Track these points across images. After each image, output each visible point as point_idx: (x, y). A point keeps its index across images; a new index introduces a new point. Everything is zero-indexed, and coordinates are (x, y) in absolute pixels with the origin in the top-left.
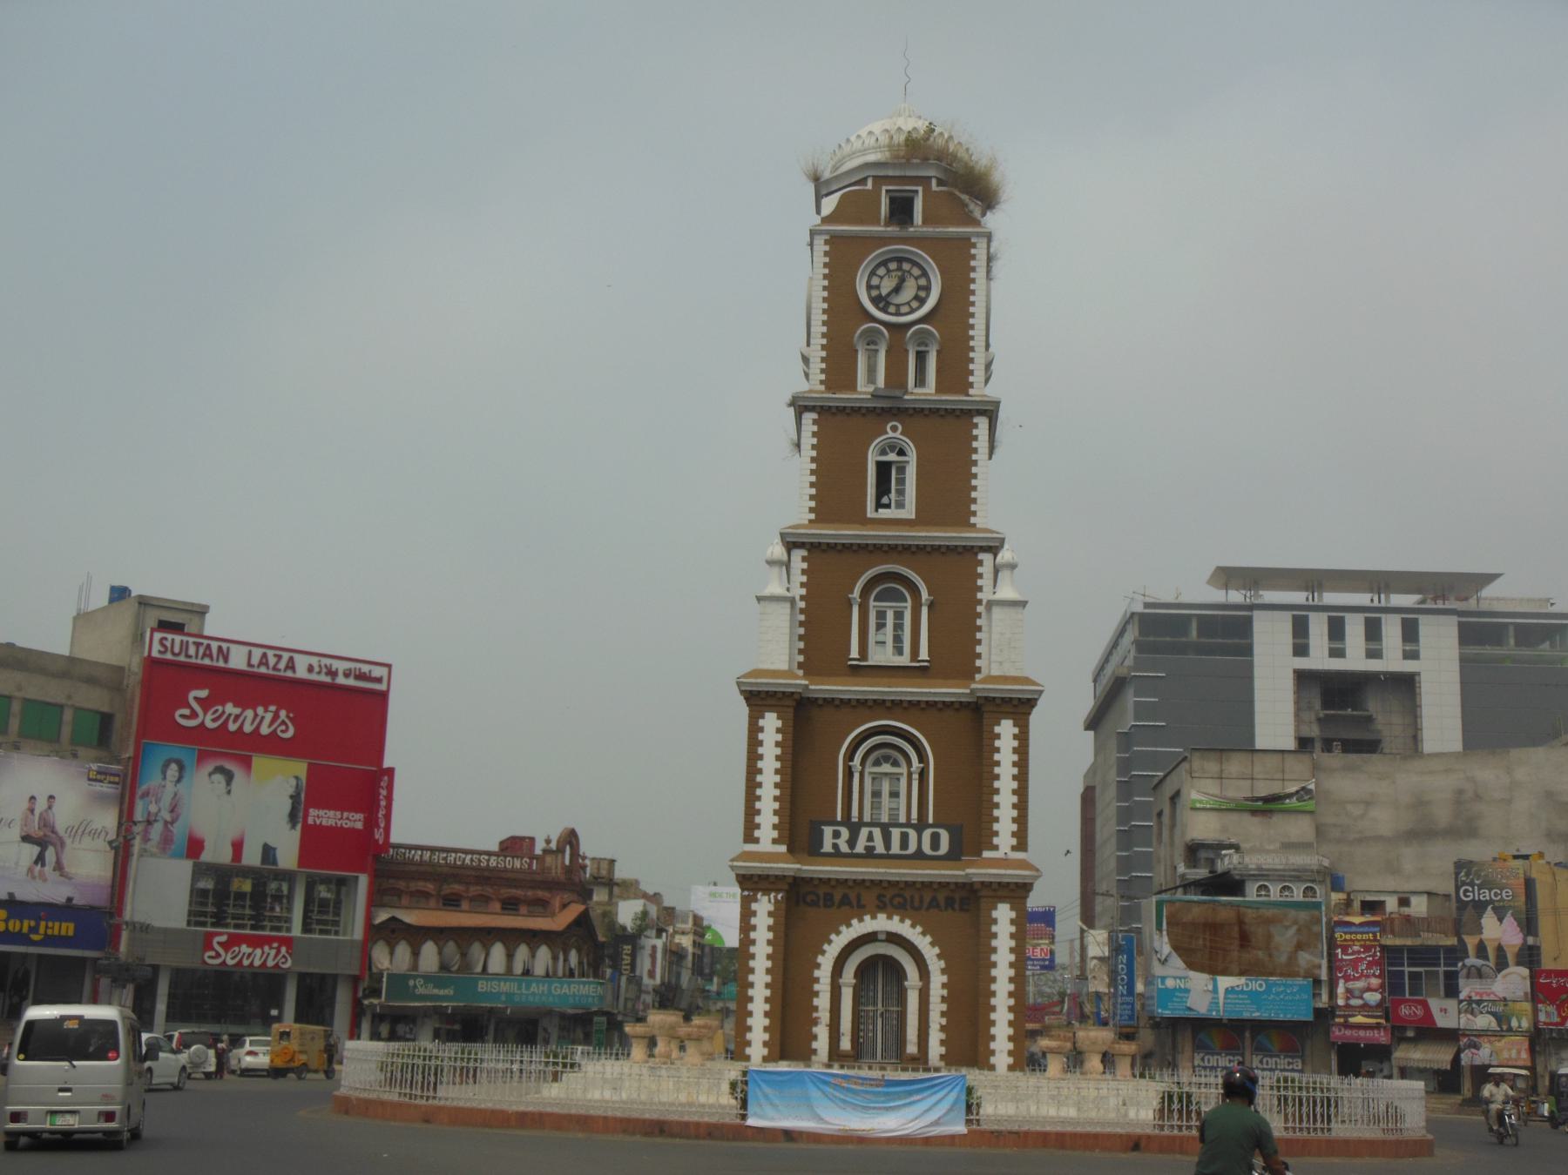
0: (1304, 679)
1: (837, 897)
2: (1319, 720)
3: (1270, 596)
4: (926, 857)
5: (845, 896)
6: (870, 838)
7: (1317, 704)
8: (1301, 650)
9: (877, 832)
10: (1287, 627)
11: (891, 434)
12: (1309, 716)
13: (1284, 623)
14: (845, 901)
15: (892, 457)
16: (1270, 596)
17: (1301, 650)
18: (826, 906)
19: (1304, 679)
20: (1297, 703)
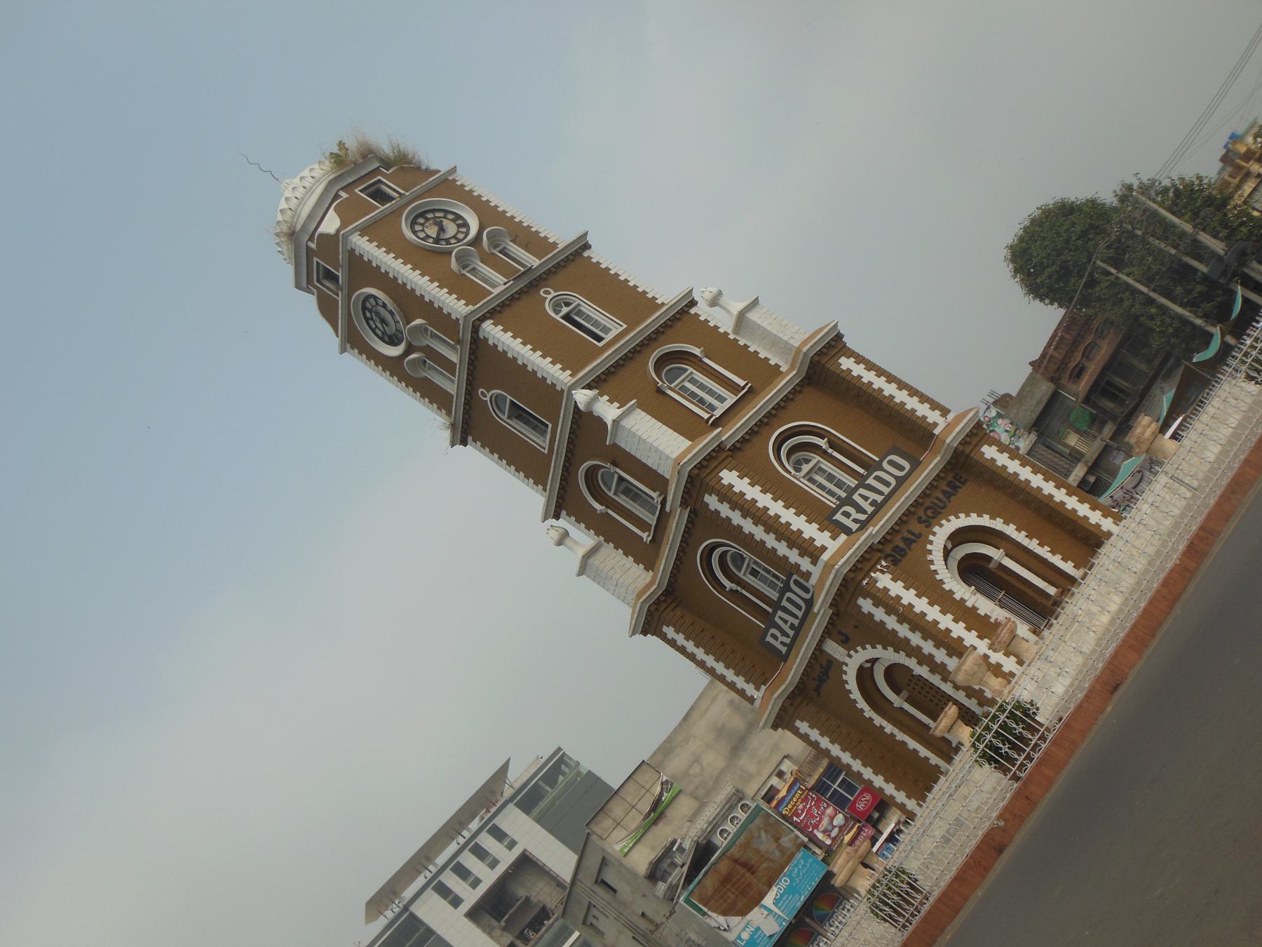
0: (473, 915)
1: (902, 545)
2: (504, 929)
3: (408, 893)
4: (898, 482)
5: (905, 540)
6: (866, 498)
7: (495, 923)
8: (456, 902)
9: (862, 491)
10: (436, 896)
11: (550, 297)
12: (497, 932)
13: (432, 897)
14: (908, 542)
15: (565, 310)
16: (408, 893)
17: (456, 902)
18: (903, 556)
19: (473, 915)
20: (484, 931)
